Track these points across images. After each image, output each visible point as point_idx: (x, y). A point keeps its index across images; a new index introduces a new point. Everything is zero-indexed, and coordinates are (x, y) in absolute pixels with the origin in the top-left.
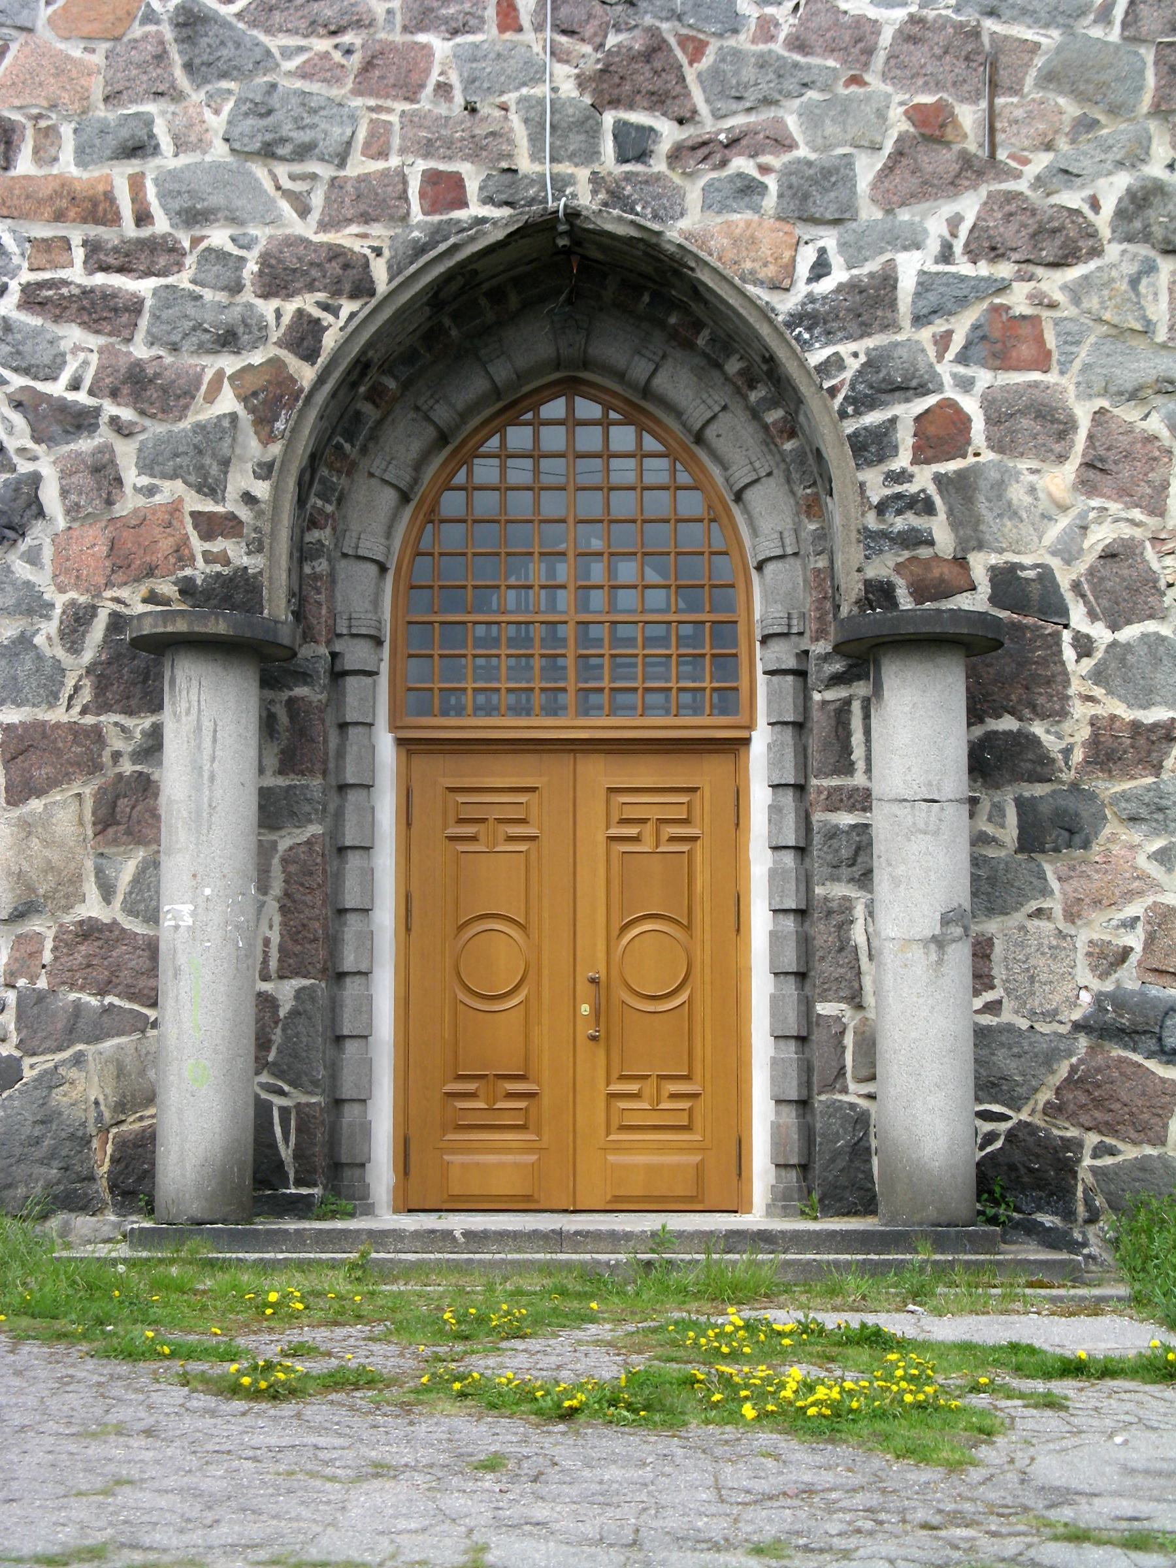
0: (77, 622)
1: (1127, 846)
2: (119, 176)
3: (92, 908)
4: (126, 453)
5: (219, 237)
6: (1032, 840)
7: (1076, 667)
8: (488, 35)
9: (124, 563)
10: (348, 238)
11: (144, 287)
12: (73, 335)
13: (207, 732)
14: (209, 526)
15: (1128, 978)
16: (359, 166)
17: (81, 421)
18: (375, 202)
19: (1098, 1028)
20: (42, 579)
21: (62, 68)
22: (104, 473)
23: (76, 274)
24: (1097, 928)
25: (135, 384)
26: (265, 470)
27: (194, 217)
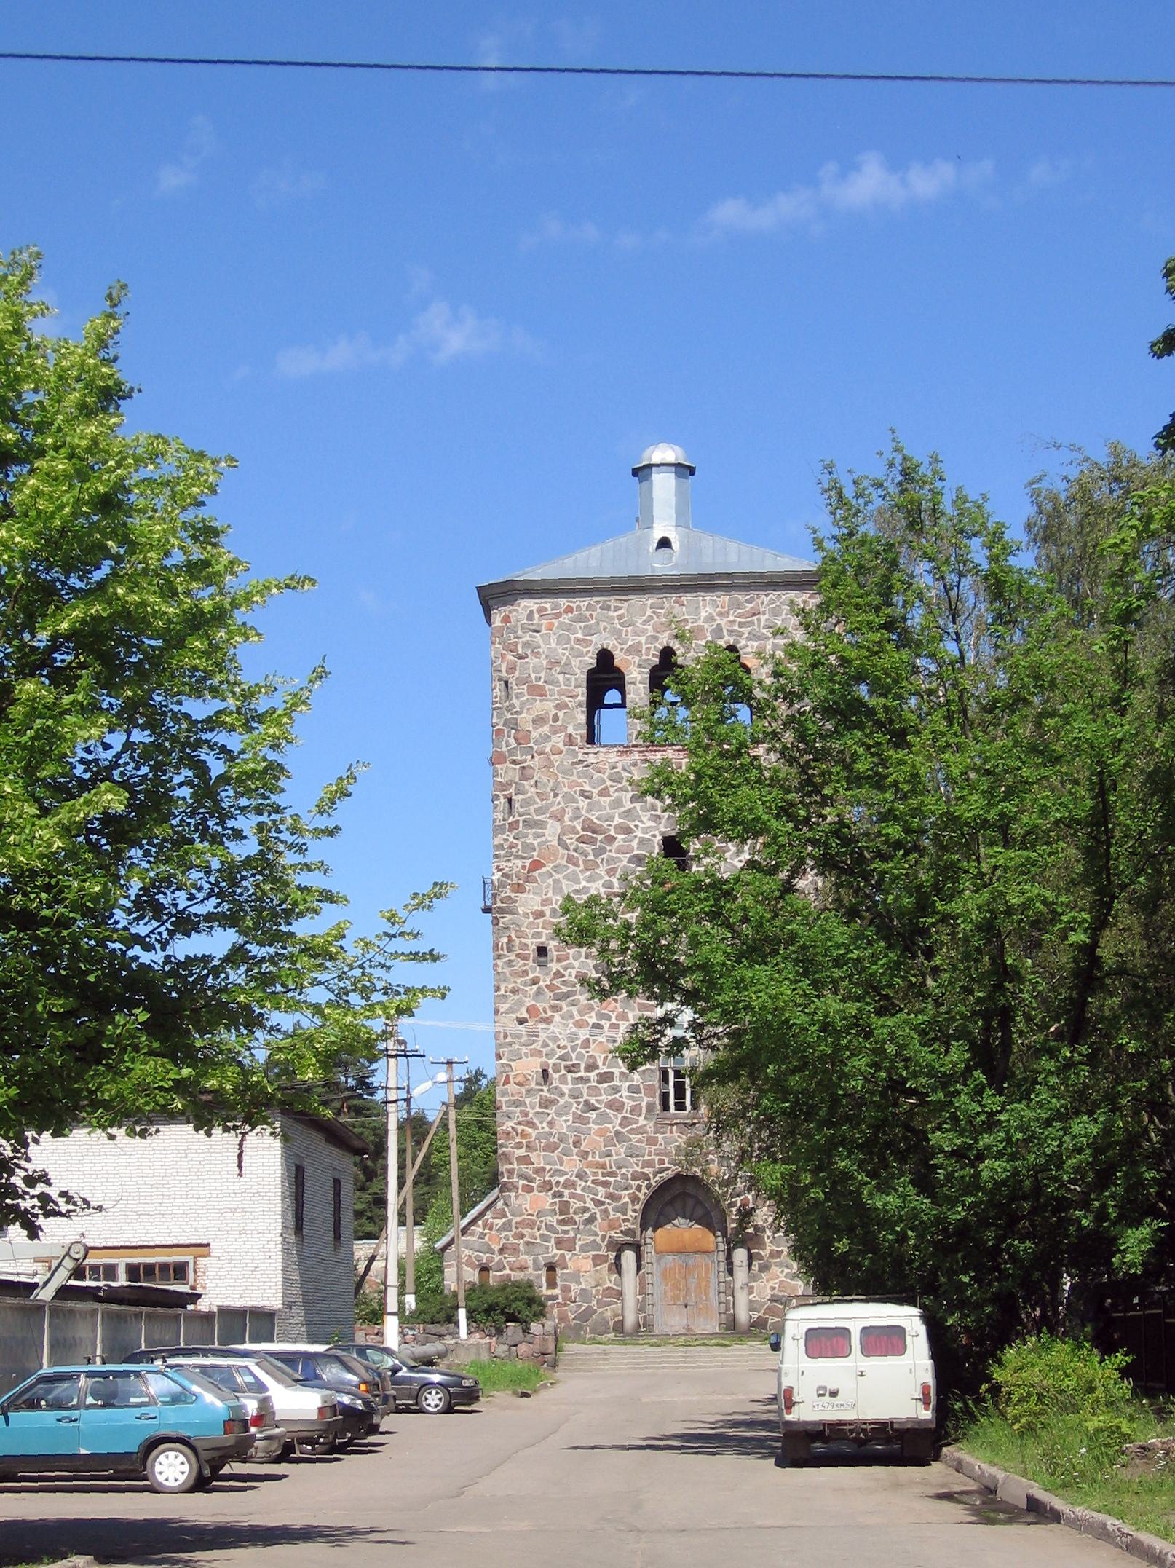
0: (603, 1238)
1: (775, 1270)
2: (607, 1159)
3: (608, 1285)
4: (610, 1208)
5: (624, 1171)
6: (760, 1270)
7: (767, 1241)
8: (668, 1135)
9: (611, 1227)
10: (645, 1170)
11: (612, 1179)
12: (600, 1188)
13: (629, 1257)
14: (624, 1220)
15: (775, 1292)
16: (647, 1158)
17: (603, 1203)
18: (649, 1164)
19: (772, 1300)
20: (597, 1230)
21: (597, 1142)
22: (606, 1211)
23: (600, 1178)
24: (771, 1284)
25: (610, 1196)
26: (634, 1211)
27: (619, 1168)
